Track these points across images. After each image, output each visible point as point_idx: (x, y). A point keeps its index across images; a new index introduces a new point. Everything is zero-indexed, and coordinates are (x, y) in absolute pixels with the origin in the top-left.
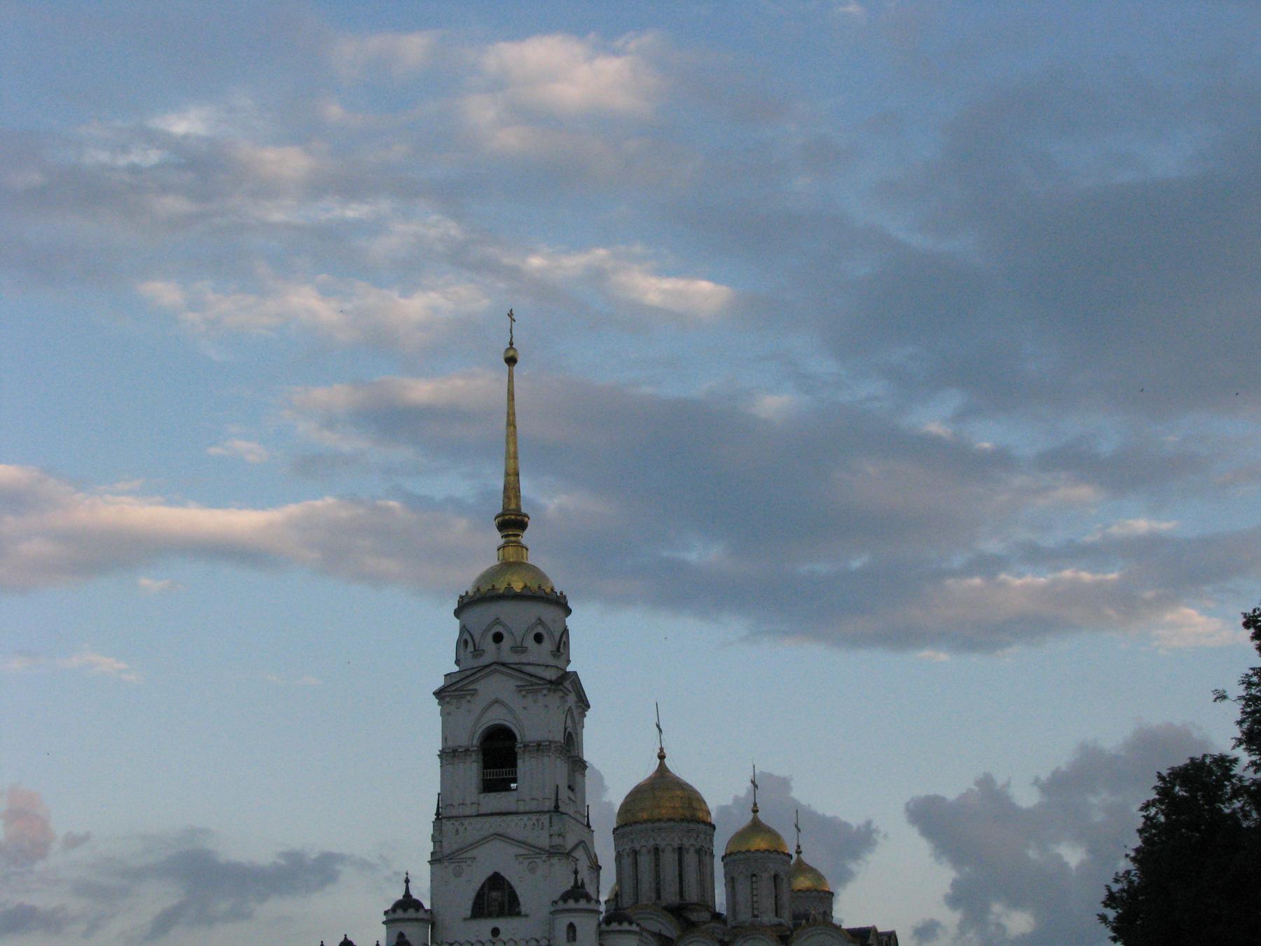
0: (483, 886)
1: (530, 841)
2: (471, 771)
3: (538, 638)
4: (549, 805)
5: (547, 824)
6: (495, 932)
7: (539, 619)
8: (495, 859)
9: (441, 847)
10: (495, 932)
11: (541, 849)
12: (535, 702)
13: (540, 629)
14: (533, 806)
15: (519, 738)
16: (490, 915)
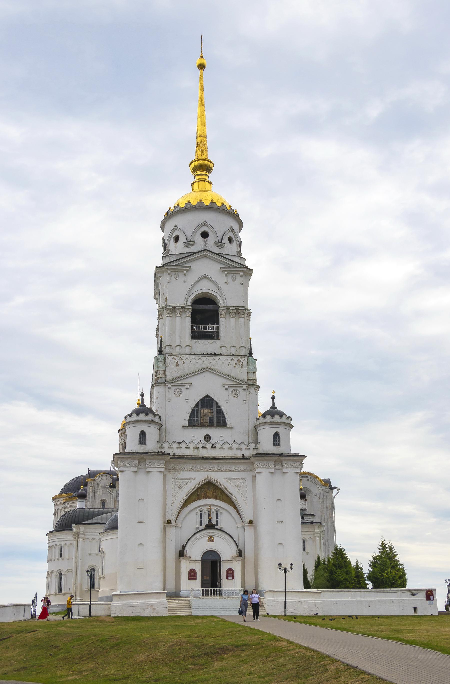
0: (197, 405)
1: (233, 375)
2: (184, 324)
3: (230, 240)
4: (244, 352)
5: (245, 363)
6: (207, 438)
7: (231, 227)
8: (207, 386)
9: (165, 374)
10: (207, 438)
11: (242, 381)
12: (234, 280)
13: (231, 234)
14: (233, 351)
15: (221, 304)
16: (203, 425)
